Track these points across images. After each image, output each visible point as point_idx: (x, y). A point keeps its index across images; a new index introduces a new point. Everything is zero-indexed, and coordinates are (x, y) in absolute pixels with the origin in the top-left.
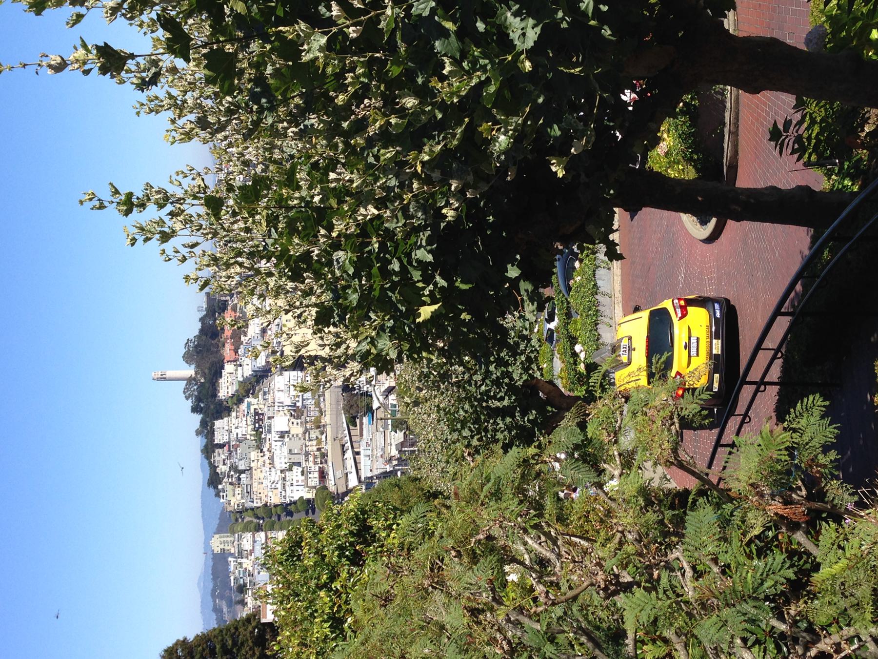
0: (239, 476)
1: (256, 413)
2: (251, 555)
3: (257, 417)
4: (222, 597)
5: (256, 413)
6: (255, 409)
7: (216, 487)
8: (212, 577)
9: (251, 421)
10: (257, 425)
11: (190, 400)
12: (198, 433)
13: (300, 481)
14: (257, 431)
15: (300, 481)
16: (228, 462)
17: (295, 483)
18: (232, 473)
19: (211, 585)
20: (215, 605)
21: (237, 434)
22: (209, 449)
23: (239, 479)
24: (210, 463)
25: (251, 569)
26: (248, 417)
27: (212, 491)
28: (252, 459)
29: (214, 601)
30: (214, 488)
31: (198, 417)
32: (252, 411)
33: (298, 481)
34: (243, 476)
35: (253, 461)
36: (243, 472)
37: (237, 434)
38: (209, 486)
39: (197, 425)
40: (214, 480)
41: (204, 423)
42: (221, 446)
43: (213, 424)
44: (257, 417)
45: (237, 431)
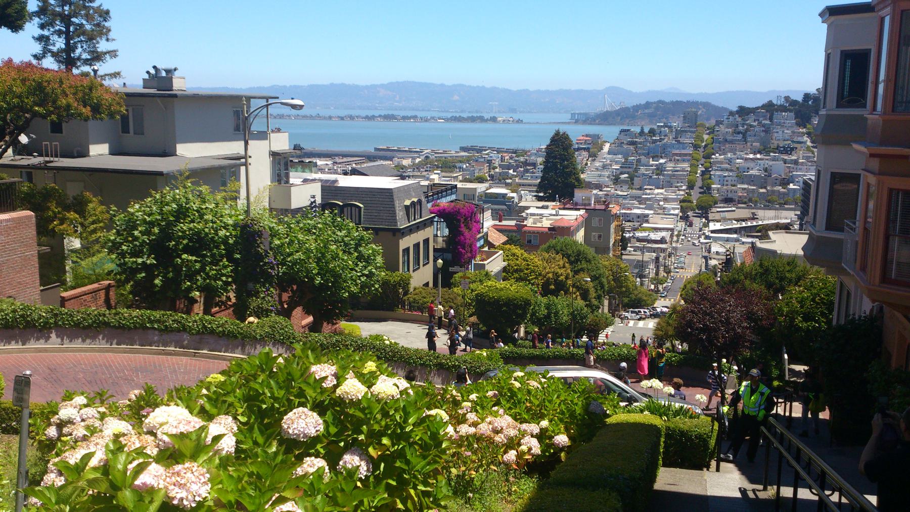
0: (742, 133)
1: (792, 149)
2: (676, 141)
3: (789, 149)
4: (657, 108)
5: (792, 149)
6: (796, 148)
7: (737, 112)
8: (674, 101)
9: (786, 145)
10: (782, 149)
11: (816, 92)
12: (787, 98)
13: (727, 183)
14: (777, 149)
15: (727, 183)
16: (755, 124)
17: (725, 179)
18: (745, 127)
19: (667, 100)
20: (652, 103)
21: (777, 132)
22: (770, 108)
23: (739, 133)
24: (757, 108)
25: (665, 141)
26: (789, 142)
27: (735, 109)
28: (754, 144)
29: (655, 103)
30: (737, 111)
31: (800, 98)
32: (796, 145)
33: (727, 181)
34: (741, 135)
35: (752, 145)
36: (744, 137)
37: (777, 132)
38: (739, 107)
39: (794, 97)
40: (743, 111)
41: (794, 103)
42: (771, 119)
43: (790, 111)
44: (789, 149)
45: (781, 132)
